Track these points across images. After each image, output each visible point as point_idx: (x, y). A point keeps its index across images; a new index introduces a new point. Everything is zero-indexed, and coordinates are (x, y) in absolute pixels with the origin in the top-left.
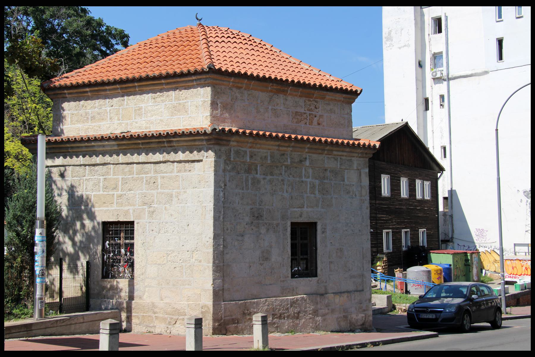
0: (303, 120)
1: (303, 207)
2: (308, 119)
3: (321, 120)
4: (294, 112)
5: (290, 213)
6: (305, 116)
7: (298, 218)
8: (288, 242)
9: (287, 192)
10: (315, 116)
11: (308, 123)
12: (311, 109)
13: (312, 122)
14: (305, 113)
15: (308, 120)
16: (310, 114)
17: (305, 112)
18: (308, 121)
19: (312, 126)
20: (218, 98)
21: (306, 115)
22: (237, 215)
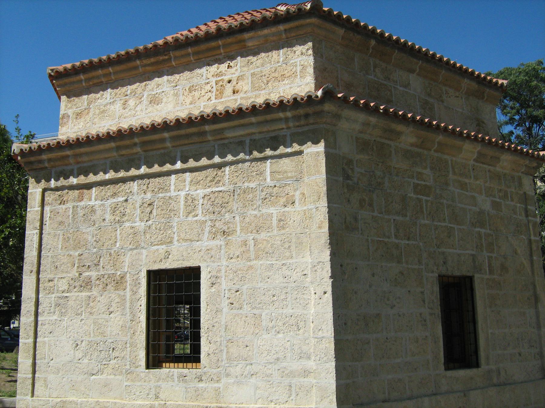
0: (203, 96)
1: (171, 242)
2: (214, 90)
3: (239, 84)
4: (187, 90)
5: (147, 256)
6: (208, 87)
7: (161, 261)
8: (141, 306)
9: (141, 220)
10: (229, 82)
11: (213, 98)
12: (220, 72)
13: (222, 93)
14: (208, 83)
15: (214, 92)
16: (217, 83)
17: (207, 81)
18: (214, 94)
19: (222, 100)
20: (71, 108)
21: (209, 85)
22: (58, 266)
